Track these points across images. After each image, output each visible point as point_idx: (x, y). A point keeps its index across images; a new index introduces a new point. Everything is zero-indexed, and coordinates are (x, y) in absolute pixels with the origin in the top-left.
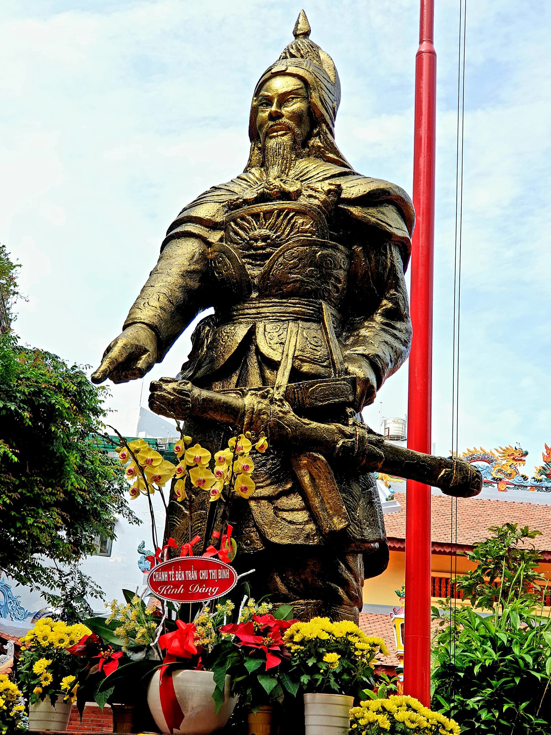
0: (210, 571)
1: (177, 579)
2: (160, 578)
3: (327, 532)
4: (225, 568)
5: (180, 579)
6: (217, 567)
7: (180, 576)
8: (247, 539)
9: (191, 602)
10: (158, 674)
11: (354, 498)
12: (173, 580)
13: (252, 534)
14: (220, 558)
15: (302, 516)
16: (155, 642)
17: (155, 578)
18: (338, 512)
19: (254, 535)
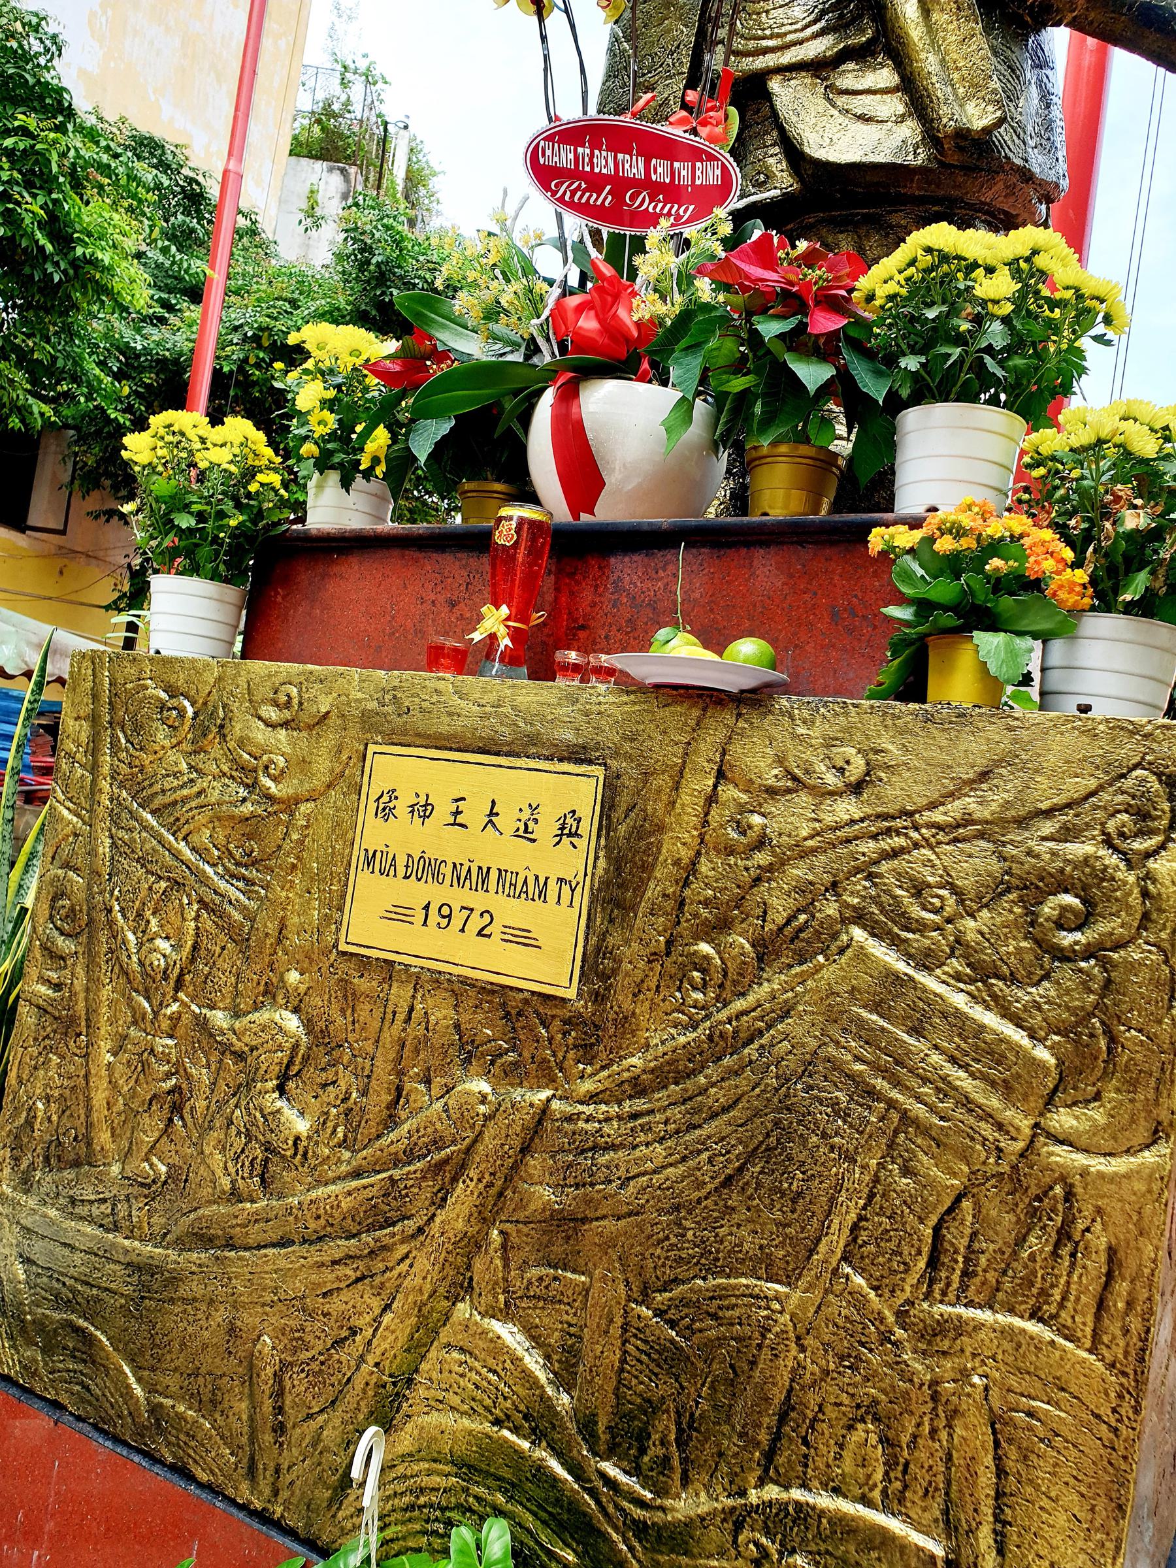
0: (676, 165)
1: (597, 170)
2: (556, 159)
3: (949, 130)
4: (711, 158)
5: (604, 171)
6: (696, 155)
7: (603, 162)
8: (759, 173)
9: (629, 232)
10: (547, 400)
11: (1013, 71)
12: (587, 169)
13: (771, 161)
14: (703, 135)
15: (895, 105)
16: (543, 317)
17: (544, 155)
18: (976, 88)
19: (776, 163)
